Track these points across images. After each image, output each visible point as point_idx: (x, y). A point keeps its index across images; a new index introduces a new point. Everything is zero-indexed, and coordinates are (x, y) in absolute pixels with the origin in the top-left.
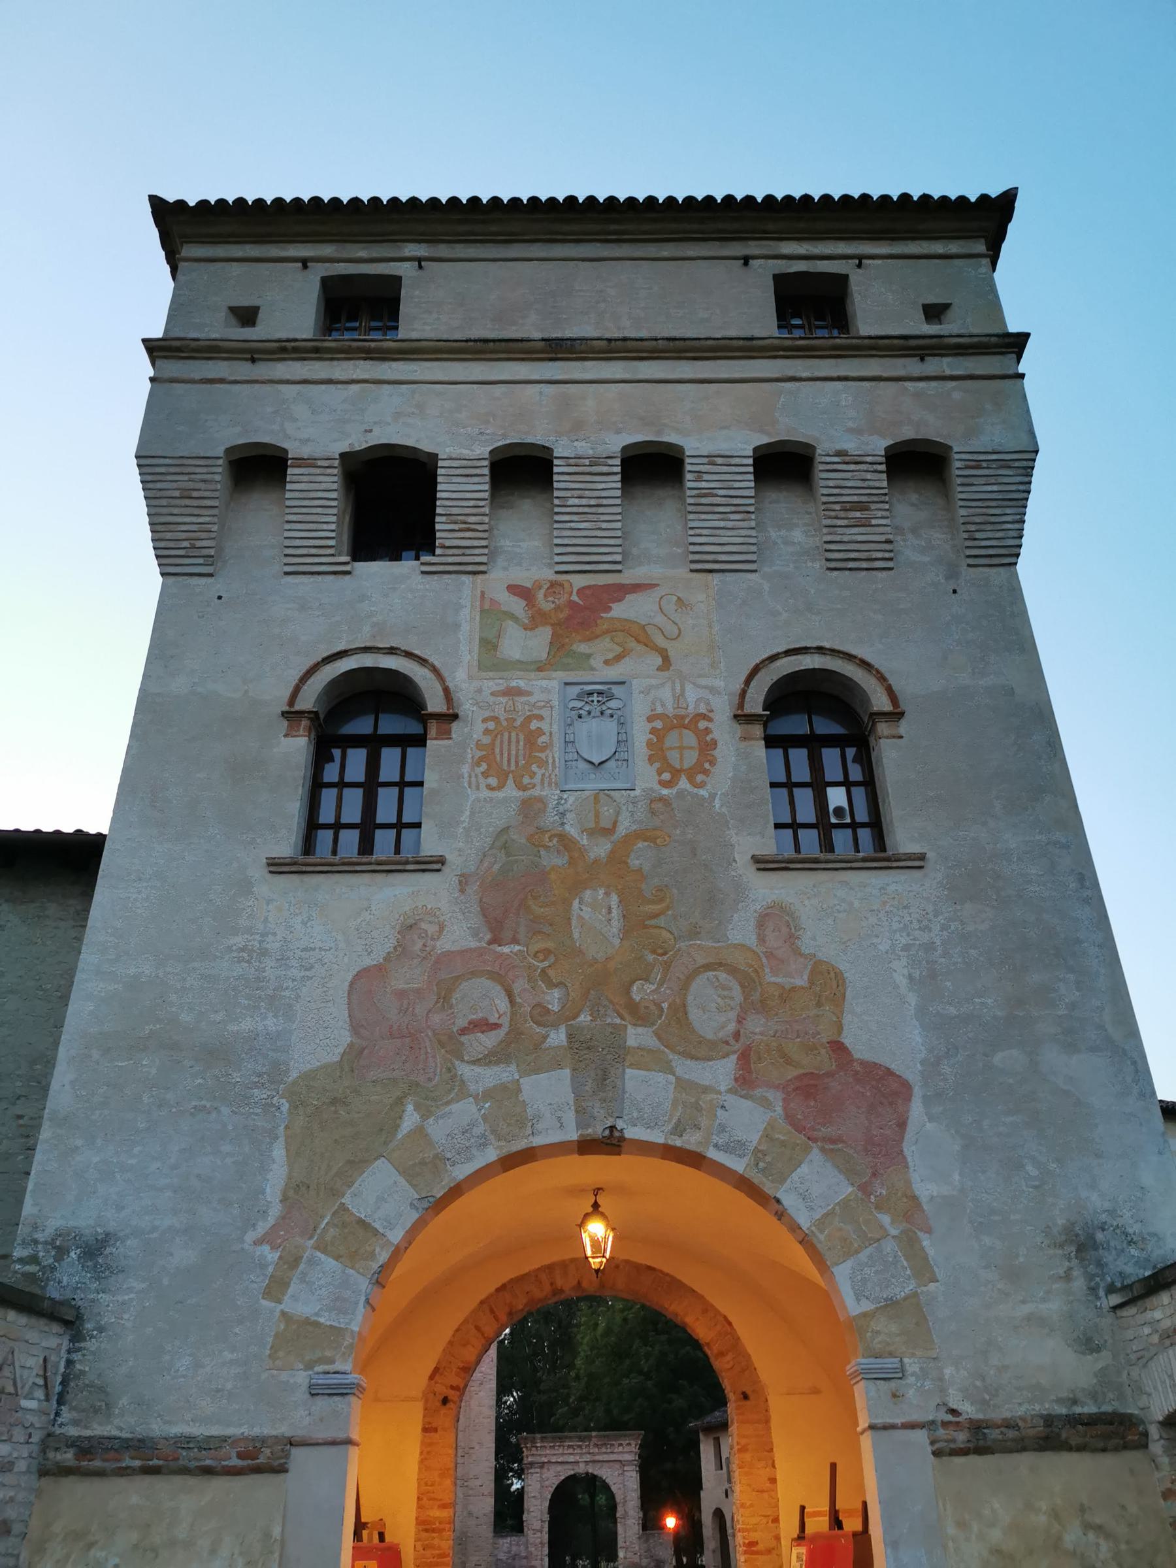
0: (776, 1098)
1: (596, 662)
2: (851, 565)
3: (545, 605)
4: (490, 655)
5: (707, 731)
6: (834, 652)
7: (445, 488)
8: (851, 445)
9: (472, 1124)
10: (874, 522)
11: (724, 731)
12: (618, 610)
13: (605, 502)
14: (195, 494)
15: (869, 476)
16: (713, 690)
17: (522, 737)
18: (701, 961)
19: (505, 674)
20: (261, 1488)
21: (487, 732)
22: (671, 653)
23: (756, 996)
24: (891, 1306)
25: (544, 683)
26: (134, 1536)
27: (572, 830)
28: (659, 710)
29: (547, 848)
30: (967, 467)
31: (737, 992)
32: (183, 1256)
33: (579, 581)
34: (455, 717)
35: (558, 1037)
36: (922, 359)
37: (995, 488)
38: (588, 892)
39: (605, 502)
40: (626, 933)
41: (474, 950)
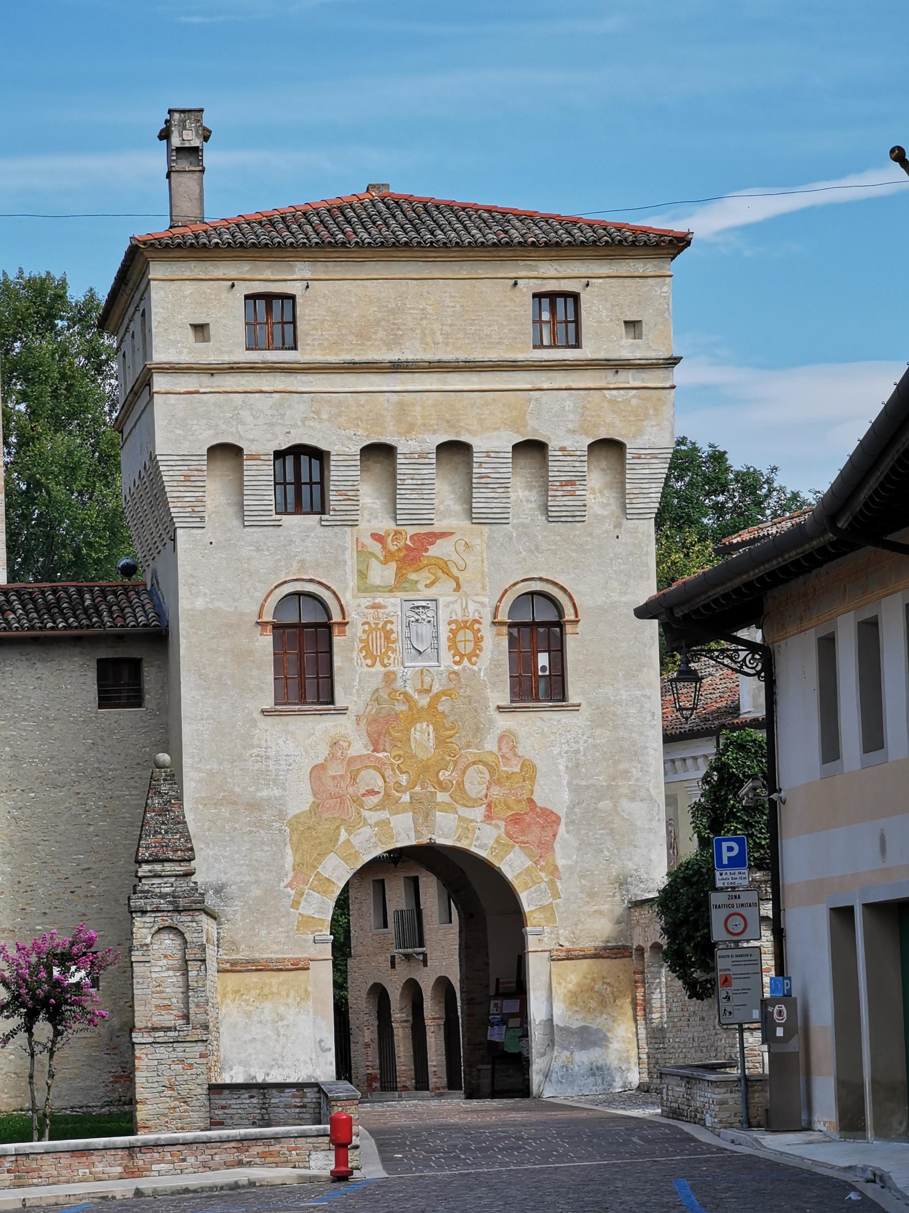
0: (502, 824)
1: (420, 586)
2: (563, 519)
3: (393, 548)
4: (365, 588)
5: (479, 630)
6: (547, 581)
7: (336, 473)
8: (567, 444)
9: (370, 837)
10: (578, 493)
11: (487, 632)
12: (434, 551)
13: (426, 481)
14: (193, 479)
15: (577, 464)
16: (482, 604)
17: (382, 634)
18: (471, 759)
19: (372, 594)
20: (301, 975)
21: (364, 631)
22: (461, 580)
23: (496, 777)
24: (542, 909)
25: (393, 600)
26: (258, 991)
27: (410, 690)
28: (454, 618)
29: (397, 700)
30: (633, 458)
31: (487, 776)
32: (256, 892)
33: (411, 531)
34: (347, 623)
35: (406, 798)
36: (617, 372)
37: (647, 471)
38: (419, 724)
39: (426, 481)
40: (437, 746)
41: (365, 755)
